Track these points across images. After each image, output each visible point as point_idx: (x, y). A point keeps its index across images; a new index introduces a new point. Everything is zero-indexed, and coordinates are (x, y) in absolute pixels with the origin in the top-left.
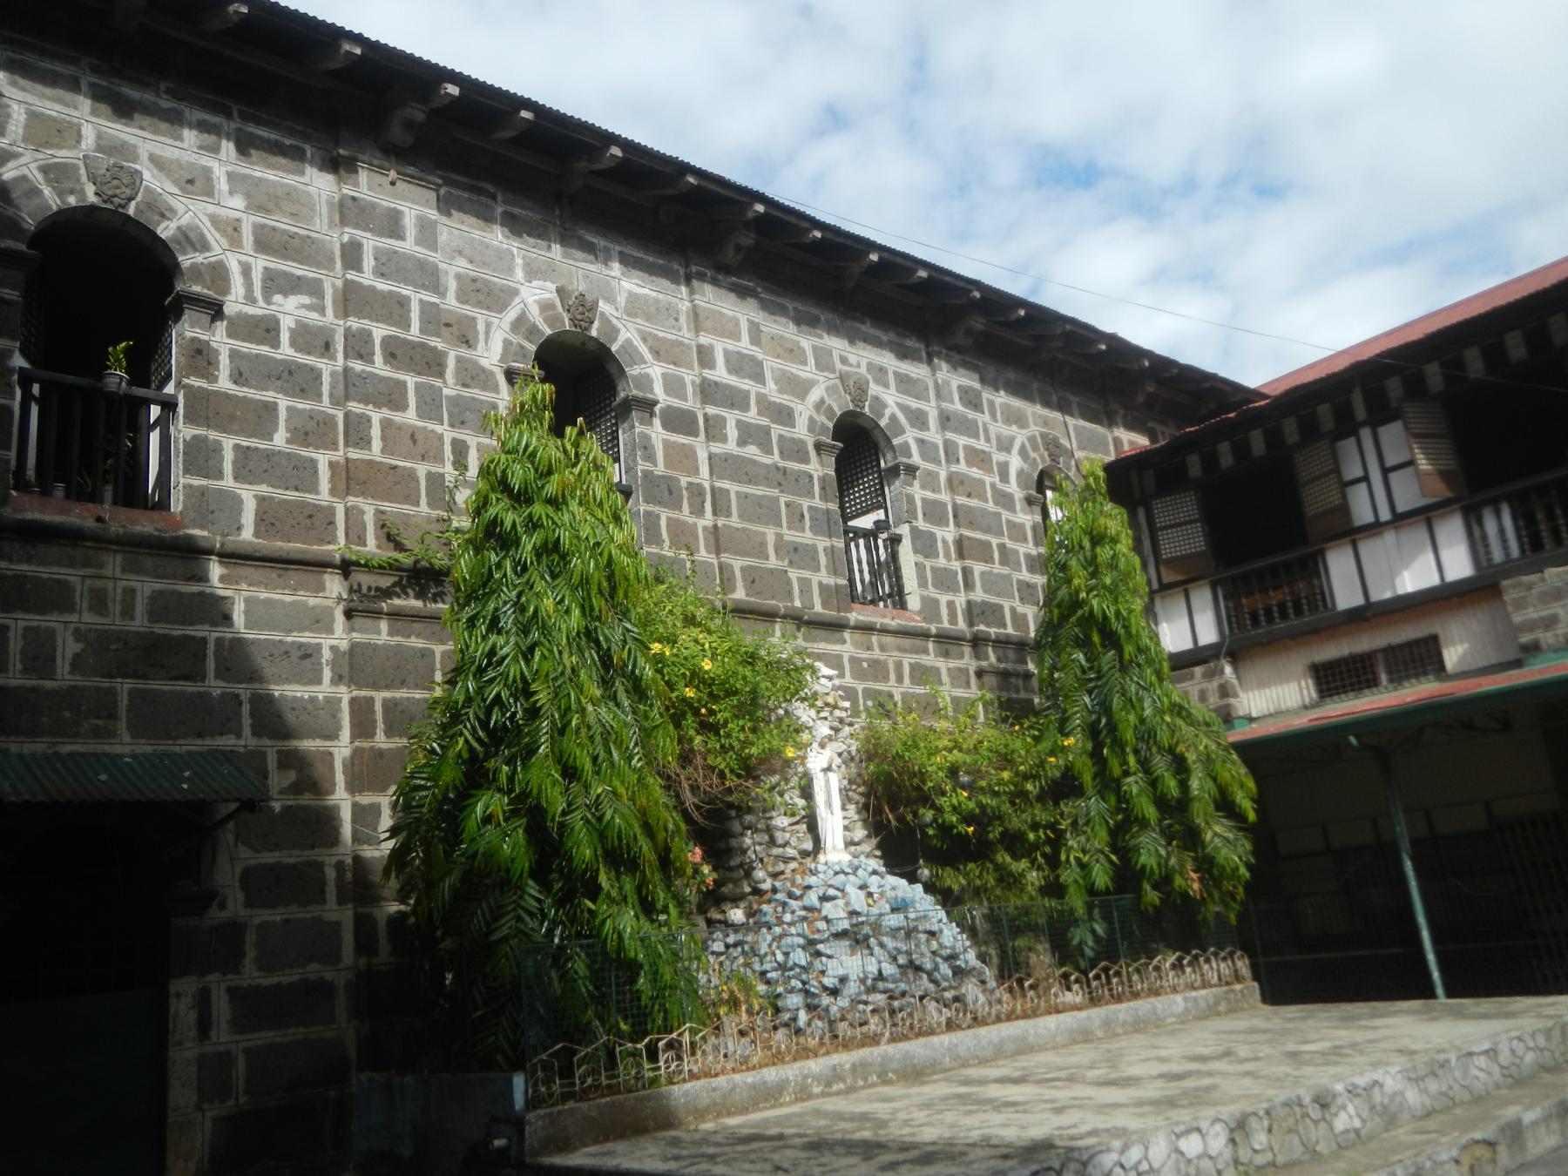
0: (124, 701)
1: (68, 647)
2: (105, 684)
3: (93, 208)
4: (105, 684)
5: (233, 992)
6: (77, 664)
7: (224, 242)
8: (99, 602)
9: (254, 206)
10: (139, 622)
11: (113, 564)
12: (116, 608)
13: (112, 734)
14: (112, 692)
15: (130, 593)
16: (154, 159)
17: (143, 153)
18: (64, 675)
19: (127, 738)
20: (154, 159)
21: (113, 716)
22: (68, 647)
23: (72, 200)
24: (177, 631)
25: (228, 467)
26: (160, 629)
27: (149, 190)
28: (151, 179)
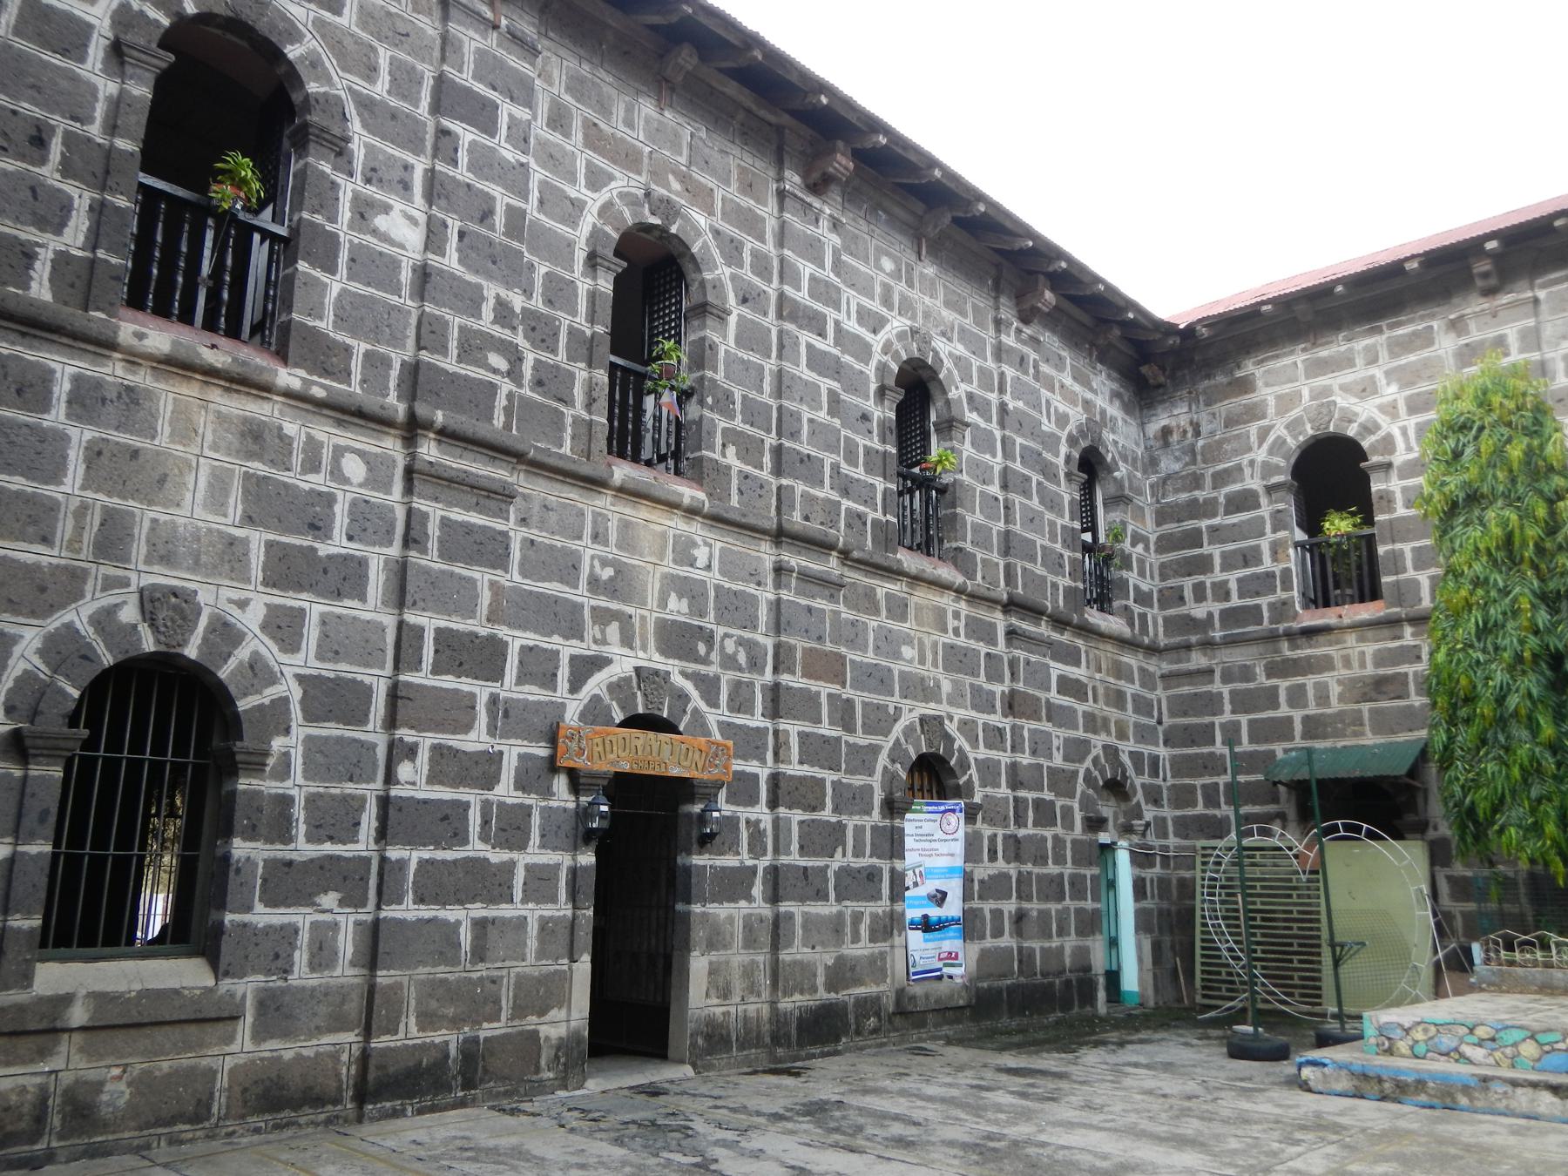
0: (1366, 715)
1: (1335, 690)
2: (1356, 706)
3: (1313, 437)
4: (1356, 706)
5: (1449, 878)
6: (1341, 698)
7: (1388, 419)
8: (1347, 662)
9: (1404, 385)
10: (1370, 670)
11: (1351, 639)
12: (1356, 664)
13: (1362, 734)
14: (1360, 711)
15: (1363, 653)
16: (1345, 388)
17: (1336, 388)
18: (1335, 706)
19: (1370, 735)
20: (1345, 388)
21: (1362, 724)
22: (1335, 690)
23: (1301, 438)
24: (1390, 671)
25: (1409, 563)
26: (1382, 671)
27: (1342, 409)
28: (1343, 401)
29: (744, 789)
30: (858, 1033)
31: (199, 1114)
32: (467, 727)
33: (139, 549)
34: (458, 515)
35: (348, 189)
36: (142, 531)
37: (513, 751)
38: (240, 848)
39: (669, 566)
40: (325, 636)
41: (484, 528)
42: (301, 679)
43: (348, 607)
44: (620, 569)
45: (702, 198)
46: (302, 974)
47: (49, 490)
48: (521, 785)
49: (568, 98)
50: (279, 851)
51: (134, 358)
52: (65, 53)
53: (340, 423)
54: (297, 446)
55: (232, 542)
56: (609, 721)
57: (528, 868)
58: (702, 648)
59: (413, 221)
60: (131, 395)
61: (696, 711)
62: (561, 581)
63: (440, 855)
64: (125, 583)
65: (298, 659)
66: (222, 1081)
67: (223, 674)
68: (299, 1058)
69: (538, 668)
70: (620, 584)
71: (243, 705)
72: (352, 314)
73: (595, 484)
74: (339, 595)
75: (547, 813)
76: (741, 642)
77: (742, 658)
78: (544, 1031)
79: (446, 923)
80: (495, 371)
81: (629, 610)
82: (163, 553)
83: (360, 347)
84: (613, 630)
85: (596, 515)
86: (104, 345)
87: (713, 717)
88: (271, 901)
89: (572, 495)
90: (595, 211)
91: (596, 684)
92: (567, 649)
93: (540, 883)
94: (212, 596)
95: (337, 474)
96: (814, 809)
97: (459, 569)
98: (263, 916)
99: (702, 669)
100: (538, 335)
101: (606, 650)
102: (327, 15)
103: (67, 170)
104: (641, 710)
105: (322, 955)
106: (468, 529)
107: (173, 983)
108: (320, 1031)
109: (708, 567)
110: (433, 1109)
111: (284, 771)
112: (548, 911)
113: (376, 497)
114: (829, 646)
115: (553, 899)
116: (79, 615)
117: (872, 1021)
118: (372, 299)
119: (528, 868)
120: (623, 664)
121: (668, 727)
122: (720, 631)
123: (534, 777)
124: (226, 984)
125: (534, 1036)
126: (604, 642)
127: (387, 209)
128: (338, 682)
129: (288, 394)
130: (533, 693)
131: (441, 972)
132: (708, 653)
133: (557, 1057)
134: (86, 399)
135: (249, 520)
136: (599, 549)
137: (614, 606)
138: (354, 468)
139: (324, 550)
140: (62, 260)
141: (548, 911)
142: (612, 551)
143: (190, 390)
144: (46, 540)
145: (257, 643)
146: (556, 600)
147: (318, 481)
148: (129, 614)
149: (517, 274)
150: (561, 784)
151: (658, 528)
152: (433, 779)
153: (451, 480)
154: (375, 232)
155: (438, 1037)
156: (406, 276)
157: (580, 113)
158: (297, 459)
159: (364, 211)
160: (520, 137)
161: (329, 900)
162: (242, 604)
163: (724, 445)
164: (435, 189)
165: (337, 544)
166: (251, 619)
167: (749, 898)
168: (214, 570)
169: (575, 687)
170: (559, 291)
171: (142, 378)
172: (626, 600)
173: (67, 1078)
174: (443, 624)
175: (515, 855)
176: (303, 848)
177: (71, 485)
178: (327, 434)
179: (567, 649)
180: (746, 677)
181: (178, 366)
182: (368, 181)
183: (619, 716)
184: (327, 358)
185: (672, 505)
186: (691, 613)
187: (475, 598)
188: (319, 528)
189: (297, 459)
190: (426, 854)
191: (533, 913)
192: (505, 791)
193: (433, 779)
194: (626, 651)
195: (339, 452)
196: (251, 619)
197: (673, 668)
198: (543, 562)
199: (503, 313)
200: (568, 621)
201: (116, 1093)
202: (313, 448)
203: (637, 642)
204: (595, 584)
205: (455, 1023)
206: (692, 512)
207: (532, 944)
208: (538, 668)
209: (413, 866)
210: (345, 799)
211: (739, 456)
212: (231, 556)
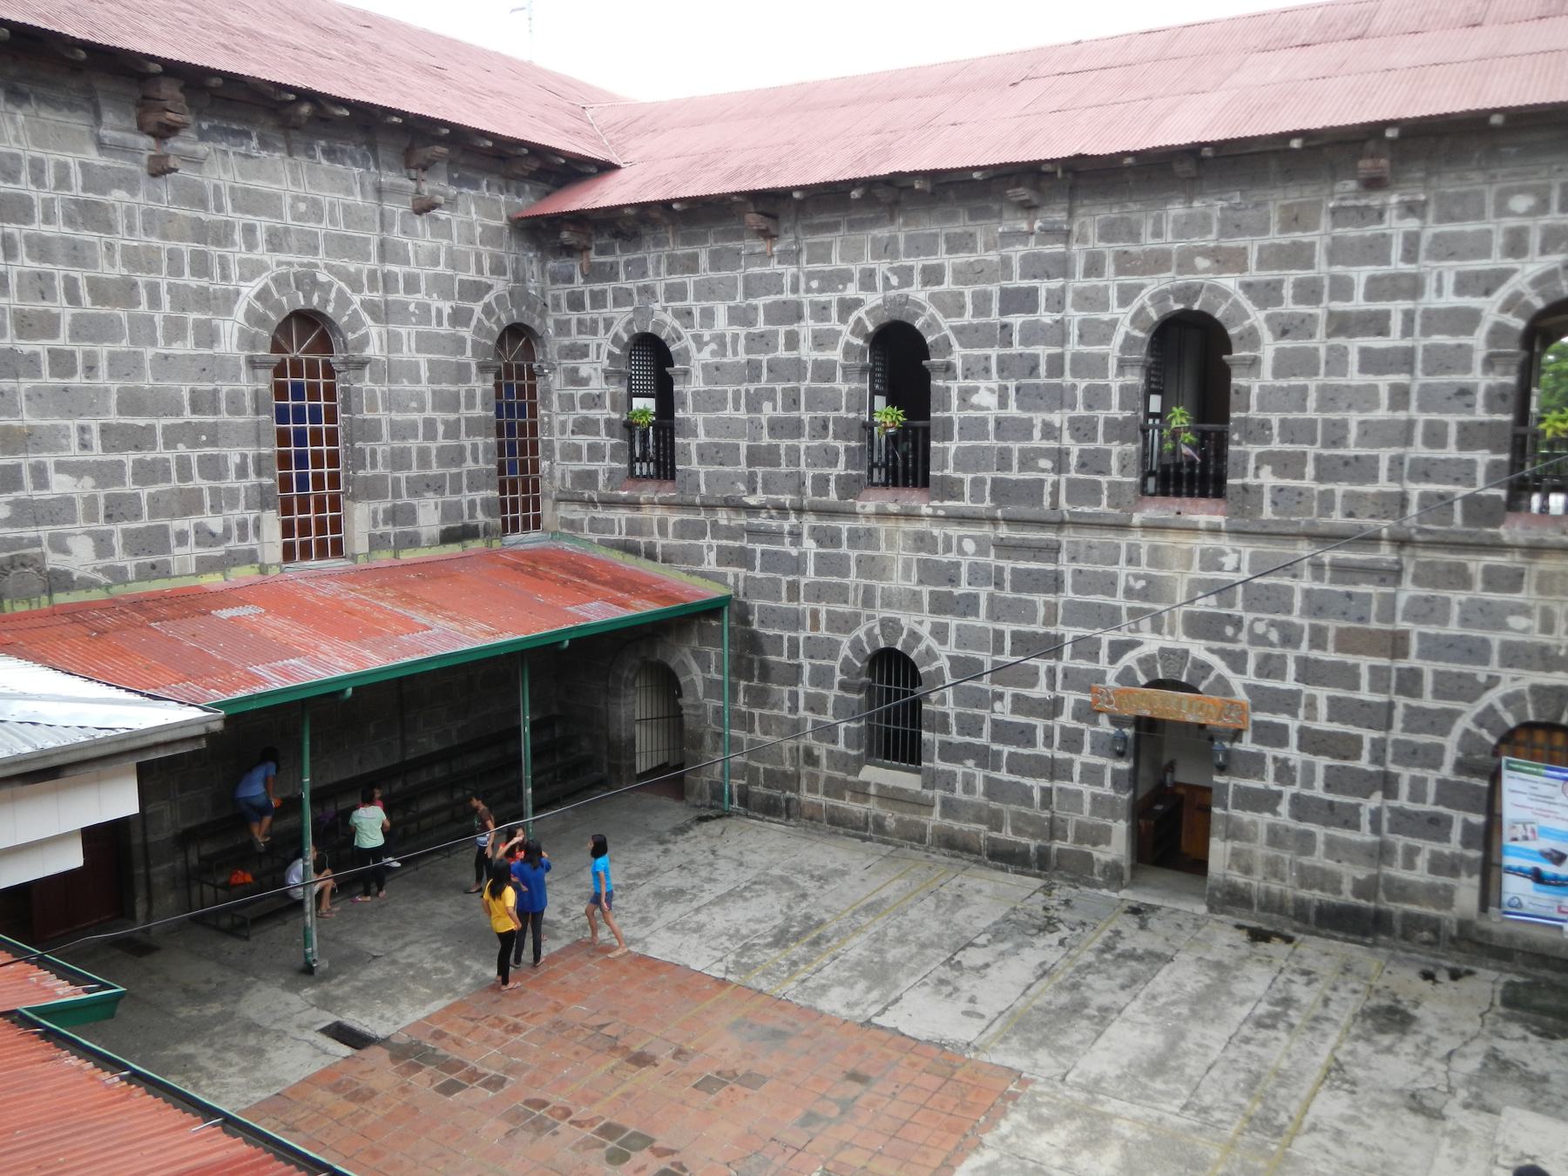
29: (1276, 735)
30: (1405, 937)
31: (921, 840)
32: (1033, 685)
33: (878, 602)
34: (1022, 565)
35: (954, 386)
36: (878, 594)
37: (1071, 698)
38: (926, 735)
39: (1196, 573)
40: (959, 636)
41: (1039, 571)
42: (949, 657)
43: (970, 621)
44: (1150, 580)
45: (1230, 260)
46: (959, 794)
47: (845, 581)
48: (1077, 716)
49: (1102, 244)
50: (944, 737)
51: (867, 516)
52: (828, 380)
53: (960, 524)
54: (940, 541)
55: (915, 593)
56: (1135, 683)
57: (1083, 764)
58: (1229, 631)
59: (991, 391)
60: (870, 533)
61: (1220, 678)
62: (1103, 593)
63: (1021, 751)
64: (873, 617)
65: (947, 648)
66: (929, 830)
67: (912, 656)
68: (961, 830)
69: (1086, 648)
70: (1153, 589)
71: (922, 670)
72: (966, 460)
73: (1123, 527)
74: (965, 615)
75: (1095, 735)
76: (1273, 624)
77: (1274, 636)
78: (1096, 854)
79: (1025, 786)
80: (1043, 470)
81: (1160, 607)
82: (887, 604)
83: (968, 477)
84: (1146, 623)
85: (1130, 546)
86: (852, 514)
87: (1236, 682)
88: (943, 758)
89: (1110, 537)
90: (1127, 323)
91: (1129, 659)
92: (1107, 637)
93: (1092, 774)
94: (907, 620)
95: (961, 551)
96: (1345, 758)
97: (1024, 596)
98: (940, 765)
99: (1229, 646)
100: (1081, 432)
101: (1137, 637)
102: (936, 289)
103: (836, 437)
104: (1161, 676)
105: (969, 787)
106: (1029, 572)
107: (904, 786)
108: (969, 821)
109: (1237, 569)
110: (1023, 873)
111: (943, 701)
112: (1098, 790)
113: (981, 560)
114: (1374, 625)
115: (1102, 784)
116: (860, 632)
117: (1426, 935)
118: (973, 447)
119: (1083, 764)
120: (1152, 643)
121: (1190, 688)
122: (1248, 617)
123: (1086, 713)
124: (925, 792)
125: (1089, 856)
126: (1138, 630)
127: (976, 390)
128: (967, 659)
129: (934, 516)
130: (1083, 664)
131: (1024, 809)
132: (1236, 634)
133: (1104, 872)
134: (855, 537)
135: (921, 582)
136: (1133, 569)
137: (1146, 605)
138: (969, 546)
139: (957, 591)
140: (839, 477)
141: (1098, 790)
142: (1144, 569)
143: (891, 524)
144: (846, 602)
145: (929, 641)
146: (1100, 606)
147: (952, 557)
148: (877, 631)
149: (1060, 398)
150: (1104, 720)
151: (1185, 547)
152: (1014, 711)
153: (1015, 547)
154: (973, 407)
155: (1024, 840)
156: (991, 426)
157: (1109, 249)
158: (940, 547)
159: (965, 395)
160: (1057, 302)
161: (970, 763)
162: (921, 623)
163: (1257, 468)
164: (1005, 366)
165: (964, 588)
166: (925, 631)
167: (1275, 813)
168: (908, 608)
169: (1114, 659)
170: (1096, 397)
171: (873, 524)
172: (1157, 600)
173: (874, 813)
174: (1015, 627)
175: (1073, 756)
176: (955, 737)
177: (852, 579)
178: (954, 531)
179: (1107, 637)
180: (1277, 651)
181: (882, 515)
182: (966, 377)
183: (1143, 680)
184: (950, 489)
185: (1194, 529)
186: (1220, 606)
187: (1035, 611)
188: (953, 581)
189: (940, 547)
190: (1013, 749)
191: (1088, 790)
192: (1066, 719)
193: (1014, 711)
194: (1156, 636)
195: (960, 539)
196: (925, 631)
197: (1198, 649)
198: (1085, 582)
199: (1049, 431)
200: (1110, 618)
201: (890, 823)
202: (948, 539)
203: (1165, 629)
204: (1129, 593)
205: (1033, 836)
206: (1214, 531)
207: (1087, 806)
208: (1086, 648)
209: (1005, 755)
210: (974, 716)
211: (1275, 473)
212: (914, 601)
